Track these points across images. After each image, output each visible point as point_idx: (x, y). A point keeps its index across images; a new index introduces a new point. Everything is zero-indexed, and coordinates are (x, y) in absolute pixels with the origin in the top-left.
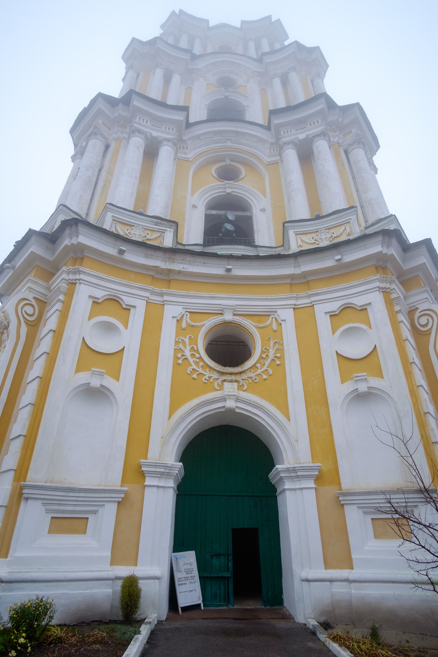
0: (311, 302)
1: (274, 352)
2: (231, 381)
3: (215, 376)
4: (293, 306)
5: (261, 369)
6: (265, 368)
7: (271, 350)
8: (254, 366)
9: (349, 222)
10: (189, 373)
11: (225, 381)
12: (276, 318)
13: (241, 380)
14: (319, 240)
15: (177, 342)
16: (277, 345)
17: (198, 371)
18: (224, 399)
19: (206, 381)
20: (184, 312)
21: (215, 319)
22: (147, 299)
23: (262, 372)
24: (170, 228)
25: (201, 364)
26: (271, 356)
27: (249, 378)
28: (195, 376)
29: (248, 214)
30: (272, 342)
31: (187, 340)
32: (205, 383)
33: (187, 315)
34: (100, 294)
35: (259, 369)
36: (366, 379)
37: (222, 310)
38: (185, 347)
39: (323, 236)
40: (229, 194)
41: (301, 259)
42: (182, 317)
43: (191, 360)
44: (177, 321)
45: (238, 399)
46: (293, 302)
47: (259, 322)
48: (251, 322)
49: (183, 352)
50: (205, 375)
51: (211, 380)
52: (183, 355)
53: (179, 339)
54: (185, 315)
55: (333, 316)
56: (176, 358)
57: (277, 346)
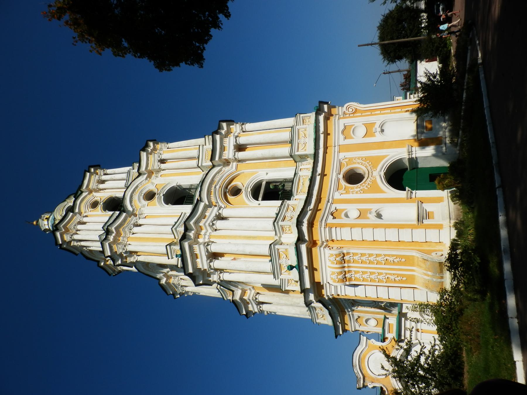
3: (369, 179)
4: (338, 153)
6: (366, 163)
7: (358, 161)
9: (299, 129)
17: (367, 185)
18: (380, 176)
19: (372, 183)
28: (369, 186)
29: (264, 183)
30: (354, 161)
31: (352, 190)
34: (331, 217)
36: (376, 128)
38: (355, 191)
39: (303, 140)
40: (251, 190)
43: (362, 188)
49: (357, 191)
51: (371, 181)
55: (345, 138)
57: (357, 159)
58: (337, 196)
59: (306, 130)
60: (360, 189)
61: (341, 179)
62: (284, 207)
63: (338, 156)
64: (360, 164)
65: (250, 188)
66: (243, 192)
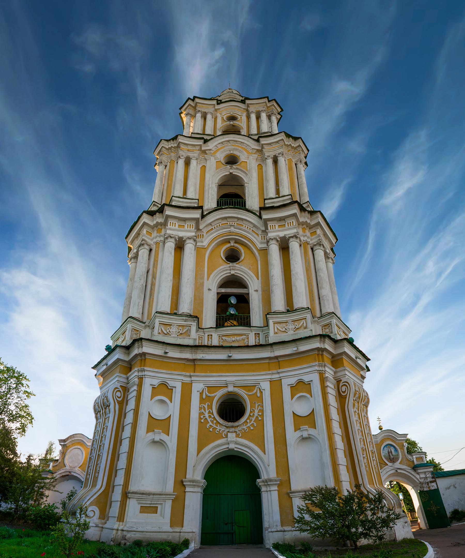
0: (280, 377)
1: (257, 411)
2: (232, 432)
4: (270, 380)
5: (250, 423)
6: (252, 422)
8: (246, 422)
9: (306, 318)
10: (208, 428)
11: (229, 432)
12: (259, 388)
13: (238, 431)
14: (287, 329)
15: (200, 408)
16: (260, 407)
17: (213, 426)
19: (218, 433)
20: (204, 387)
21: (222, 390)
22: (182, 381)
23: (250, 425)
24: (194, 322)
25: (215, 421)
26: (256, 414)
27: (242, 429)
28: (211, 430)
31: (206, 406)
32: (217, 433)
33: (206, 389)
34: (156, 382)
35: (249, 423)
37: (227, 384)
38: (205, 411)
39: (290, 327)
40: (233, 275)
41: (275, 347)
42: (203, 390)
43: (209, 420)
44: (200, 393)
45: (236, 443)
46: (269, 377)
47: (249, 391)
48: (244, 391)
49: (204, 414)
50: (217, 429)
51: (221, 432)
52: (204, 417)
53: (202, 406)
54: (205, 389)
55: (292, 387)
56: (200, 418)
58: (197, 388)
59: (305, 328)
60: (208, 418)
61: (227, 389)
62: (185, 321)
63: (264, 380)
64: (250, 413)
65: (235, 273)
66: (230, 264)
